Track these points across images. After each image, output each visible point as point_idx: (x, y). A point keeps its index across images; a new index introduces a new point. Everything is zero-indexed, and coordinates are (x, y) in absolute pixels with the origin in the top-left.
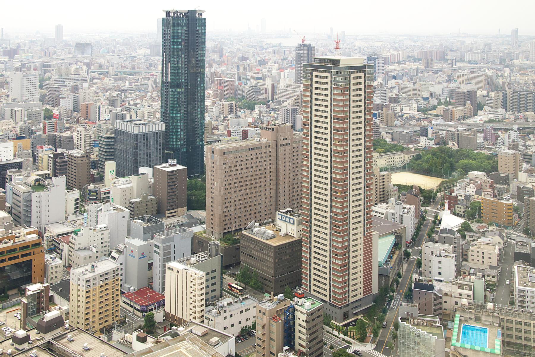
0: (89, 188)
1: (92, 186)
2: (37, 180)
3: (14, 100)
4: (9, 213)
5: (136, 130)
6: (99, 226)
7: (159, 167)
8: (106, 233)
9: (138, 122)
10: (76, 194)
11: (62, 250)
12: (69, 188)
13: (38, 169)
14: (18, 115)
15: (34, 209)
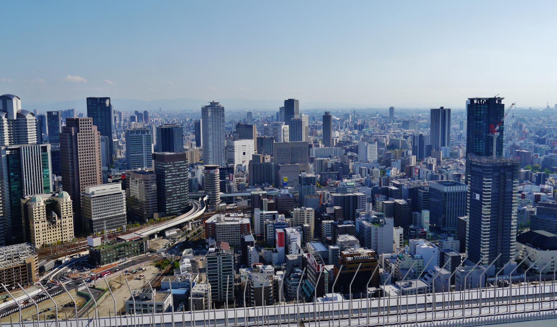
0: (410, 227)
1: (412, 226)
2: (375, 219)
3: (361, 161)
4: (357, 237)
5: (446, 189)
6: (416, 256)
7: (462, 218)
8: (421, 261)
9: (447, 183)
10: (400, 230)
11: (391, 267)
12: (396, 225)
13: (376, 210)
14: (363, 172)
15: (373, 238)
